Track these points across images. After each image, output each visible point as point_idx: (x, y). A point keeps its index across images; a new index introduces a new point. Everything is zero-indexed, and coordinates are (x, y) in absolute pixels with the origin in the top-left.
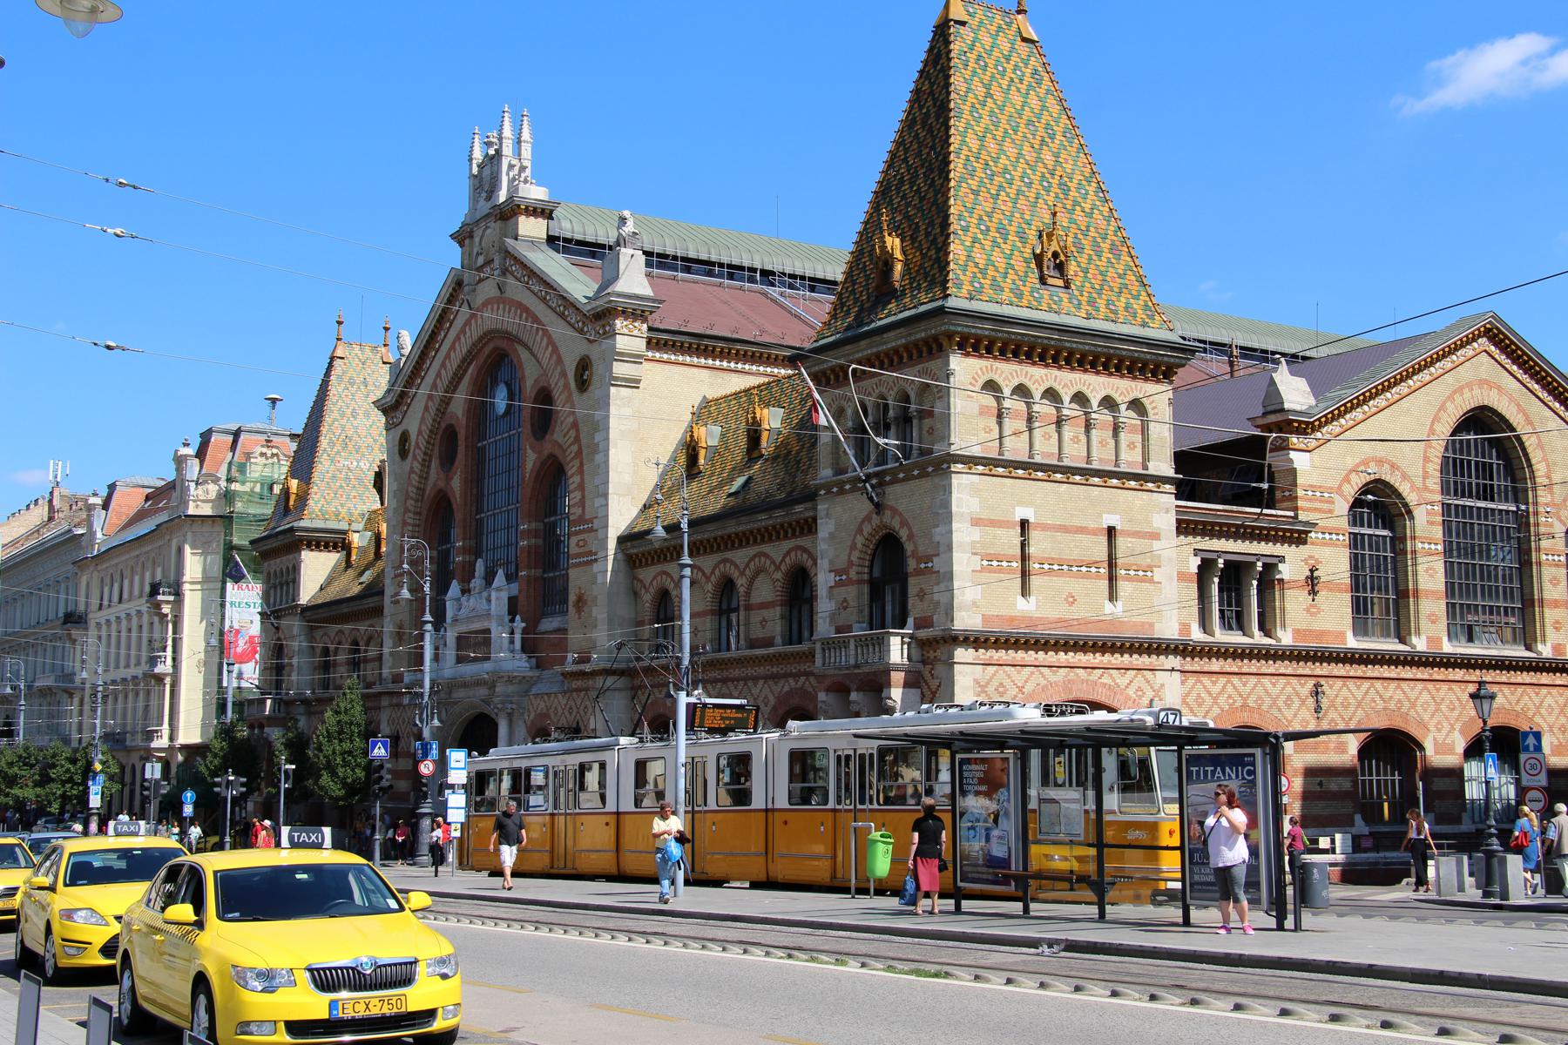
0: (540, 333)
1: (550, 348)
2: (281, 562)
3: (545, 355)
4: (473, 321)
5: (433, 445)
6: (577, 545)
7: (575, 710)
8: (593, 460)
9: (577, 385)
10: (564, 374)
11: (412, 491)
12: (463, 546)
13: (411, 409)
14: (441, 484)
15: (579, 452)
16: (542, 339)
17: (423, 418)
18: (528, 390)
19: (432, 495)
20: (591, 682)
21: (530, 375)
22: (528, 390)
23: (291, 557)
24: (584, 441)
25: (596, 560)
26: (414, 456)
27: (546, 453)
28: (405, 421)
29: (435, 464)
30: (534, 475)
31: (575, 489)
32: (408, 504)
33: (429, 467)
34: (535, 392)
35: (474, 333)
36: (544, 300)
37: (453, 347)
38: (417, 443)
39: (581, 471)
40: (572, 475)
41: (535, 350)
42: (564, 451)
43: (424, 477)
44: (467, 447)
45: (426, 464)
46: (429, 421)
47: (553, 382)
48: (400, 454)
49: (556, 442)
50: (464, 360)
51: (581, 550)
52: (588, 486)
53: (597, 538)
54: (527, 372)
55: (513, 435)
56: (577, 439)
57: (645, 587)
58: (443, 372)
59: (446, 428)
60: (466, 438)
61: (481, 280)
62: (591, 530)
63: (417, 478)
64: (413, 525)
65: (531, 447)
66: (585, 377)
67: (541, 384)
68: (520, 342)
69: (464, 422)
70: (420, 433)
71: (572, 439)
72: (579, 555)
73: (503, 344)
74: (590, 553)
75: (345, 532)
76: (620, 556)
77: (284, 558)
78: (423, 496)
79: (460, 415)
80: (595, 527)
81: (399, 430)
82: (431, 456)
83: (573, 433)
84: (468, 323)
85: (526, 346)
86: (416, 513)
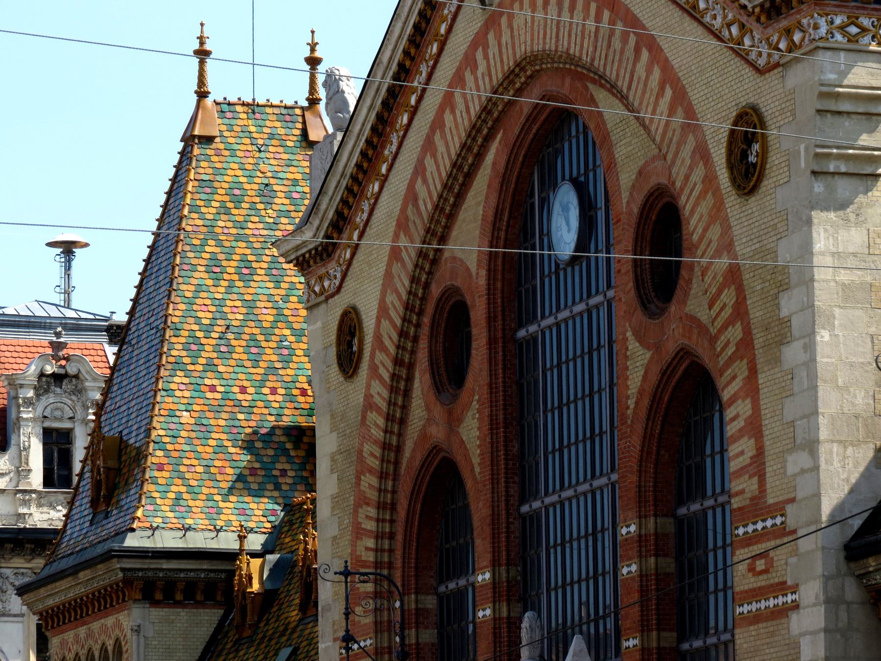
0: (645, 55)
1: (669, 92)
2: (89, 635)
4: (491, 36)
5: (415, 340)
8: (777, 360)
9: (733, 180)
10: (702, 154)
11: (372, 454)
13: (360, 256)
14: (437, 433)
16: (649, 72)
17: (388, 275)
18: (625, 195)
22: (625, 195)
23: (110, 621)
25: (795, 606)
26: (374, 368)
27: (671, 347)
28: (349, 283)
29: (421, 383)
30: (646, 402)
31: (741, 433)
32: (364, 485)
33: (407, 393)
34: (640, 198)
39: (752, 389)
40: (733, 400)
41: (634, 97)
42: (713, 339)
44: (492, 342)
46: (403, 283)
47: (679, 172)
48: (340, 365)
49: (693, 318)
50: (474, 130)
51: (761, 581)
52: (771, 428)
53: (795, 553)
54: (621, 152)
55: (597, 307)
56: (740, 312)
58: (429, 162)
62: (783, 531)
63: (381, 422)
65: (636, 334)
66: (752, 159)
67: (653, 181)
68: (602, 80)
69: (482, 282)
70: (383, 311)
71: (728, 311)
72: (757, 594)
73: (566, 87)
74: (781, 588)
75: (231, 557)
76: (852, 590)
77: (96, 626)
78: (397, 463)
79: (472, 263)
82: (411, 367)
83: (728, 297)
84: (479, 41)
85: (613, 89)
86: (381, 506)
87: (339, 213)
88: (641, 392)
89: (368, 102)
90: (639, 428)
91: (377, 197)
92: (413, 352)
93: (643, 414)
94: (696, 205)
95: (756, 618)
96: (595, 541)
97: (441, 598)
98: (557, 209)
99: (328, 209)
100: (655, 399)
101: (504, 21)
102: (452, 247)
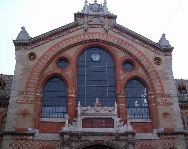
3: (135, 53)
4: (86, 35)
5: (52, 60)
6: (162, 100)
7: (167, 144)
10: (147, 59)
15: (159, 78)
17: (48, 51)
20: (175, 136)
21: (121, 55)
24: (160, 75)
25: (173, 105)
26: (40, 60)
31: (158, 86)
35: (87, 37)
36: (132, 40)
37: (72, 38)
38: (42, 57)
46: (53, 54)
57: (183, 114)
59: (61, 57)
61: (90, 27)
67: (128, 58)
70: (45, 54)
78: (43, 73)
80: (170, 96)
81: (28, 52)
83: (154, 73)
89: (50, 32)
91: (45, 43)
95: (161, 105)
101: (90, 35)
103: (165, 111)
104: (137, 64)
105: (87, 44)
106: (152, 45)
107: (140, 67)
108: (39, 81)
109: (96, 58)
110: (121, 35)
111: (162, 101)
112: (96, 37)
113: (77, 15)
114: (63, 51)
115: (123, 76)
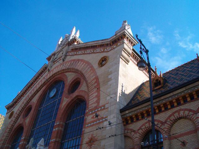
5: (22, 112)
12: (24, 139)
15: (98, 84)
19: (17, 126)
22: (68, 82)
30: (66, 105)
31: (94, 98)
32: (7, 130)
33: (18, 119)
38: (16, 113)
43: (15, 122)
44: (35, 109)
45: (17, 118)
50: (42, 85)
57: (134, 131)
60: (35, 107)
62: (104, 109)
64: (6, 136)
70: (18, 110)
74: (102, 118)
76: (120, 118)
87: (16, 101)
88: (65, 105)
90: (64, 109)
92: (21, 114)
93: (65, 106)
94: (88, 73)
96: (46, 131)
97: (12, 146)
98: (53, 90)
99: (15, 100)
100: (68, 104)
102: (32, 101)
103: (92, 135)
104: (82, 80)
105: (49, 83)
106: (100, 45)
107: (84, 82)
108: (8, 137)
109: (52, 94)
110: (76, 55)
111: (92, 120)
112: (55, 71)
113: (49, 59)
114: (31, 100)
115: (65, 101)
